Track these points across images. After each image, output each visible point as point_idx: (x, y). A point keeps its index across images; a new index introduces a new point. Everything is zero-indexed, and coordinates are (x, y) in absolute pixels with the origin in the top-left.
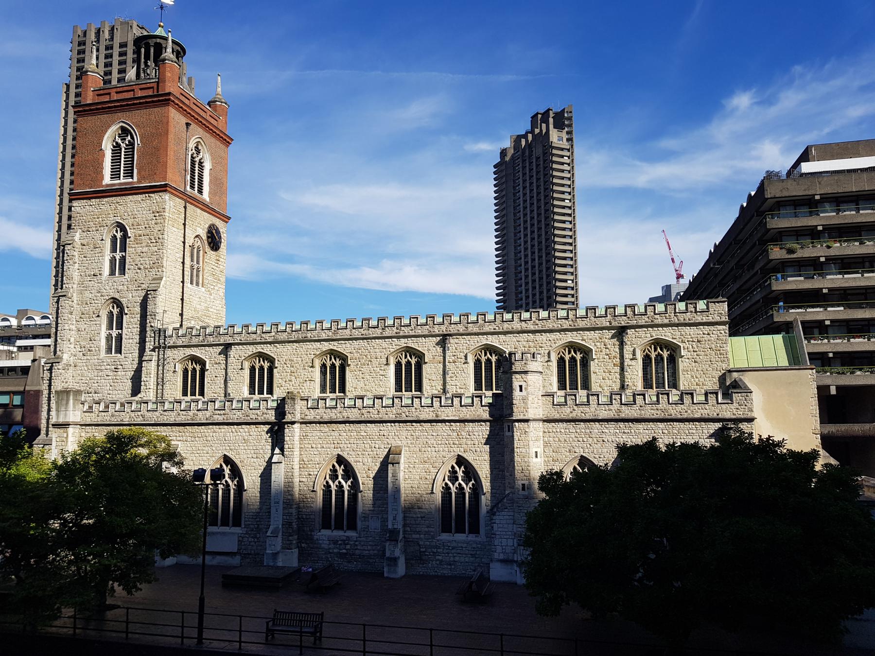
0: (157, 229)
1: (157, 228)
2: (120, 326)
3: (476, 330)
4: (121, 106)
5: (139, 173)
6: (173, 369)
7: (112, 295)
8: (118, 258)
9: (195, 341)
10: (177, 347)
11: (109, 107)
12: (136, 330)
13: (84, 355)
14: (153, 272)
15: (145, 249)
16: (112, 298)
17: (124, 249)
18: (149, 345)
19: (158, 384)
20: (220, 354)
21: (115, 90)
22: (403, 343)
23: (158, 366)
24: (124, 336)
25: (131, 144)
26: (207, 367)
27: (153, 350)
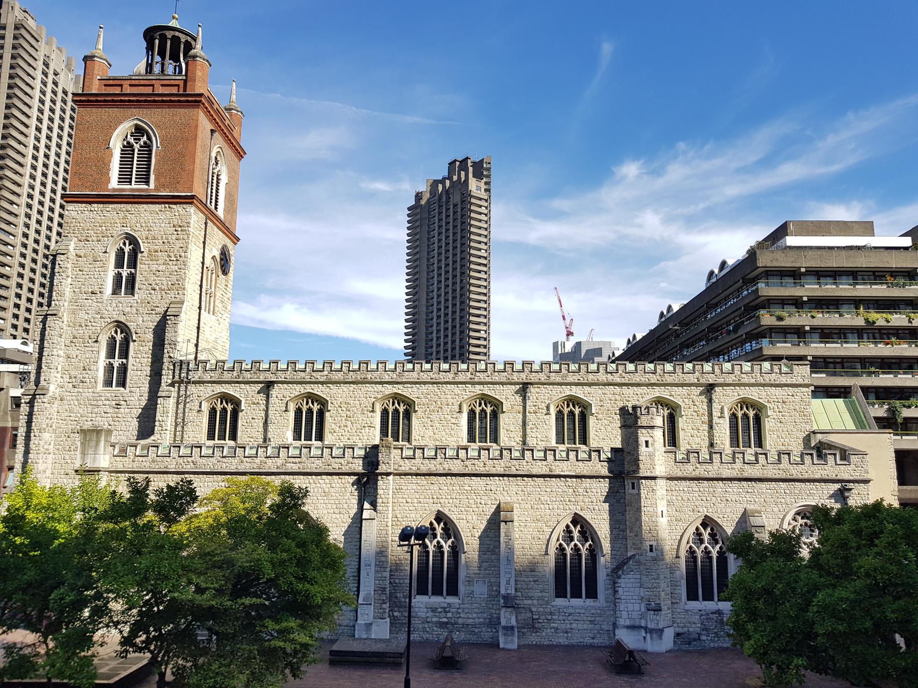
0: (178, 246)
1: (179, 244)
2: (125, 354)
4: (138, 101)
5: (156, 179)
6: (197, 408)
7: (116, 318)
8: (124, 274)
9: (227, 376)
10: (203, 382)
11: (121, 101)
12: (147, 360)
13: (74, 387)
14: (172, 294)
15: (161, 268)
16: (116, 321)
17: (133, 264)
18: (166, 378)
19: (176, 425)
20: (259, 393)
21: (129, 82)
22: (478, 390)
23: (178, 403)
24: (130, 367)
25: (148, 147)
26: (243, 408)
27: (172, 385)
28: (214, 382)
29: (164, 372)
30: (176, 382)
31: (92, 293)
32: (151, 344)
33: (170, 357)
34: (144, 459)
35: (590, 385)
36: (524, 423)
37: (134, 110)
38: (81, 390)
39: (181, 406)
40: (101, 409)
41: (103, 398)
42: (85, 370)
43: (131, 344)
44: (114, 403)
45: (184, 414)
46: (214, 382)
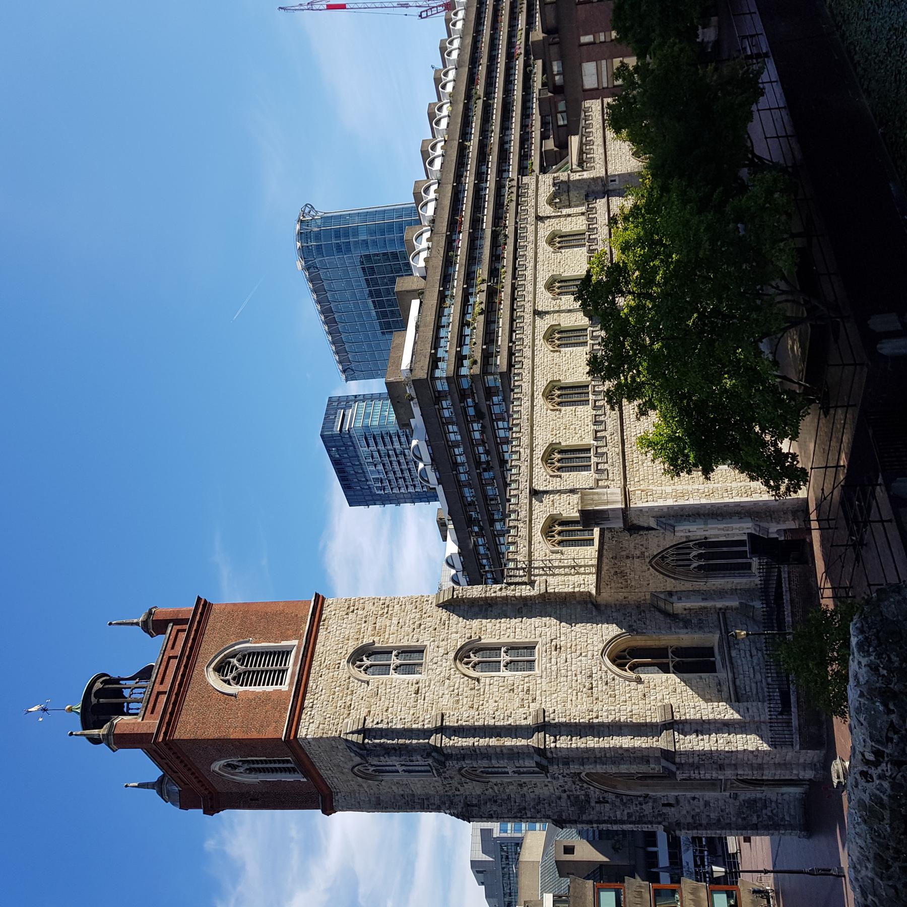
1: (369, 606)
2: (495, 649)
3: (531, 296)
4: (186, 667)
6: (558, 556)
7: (450, 662)
10: (530, 553)
11: (180, 685)
13: (534, 700)
14: (426, 607)
16: (455, 659)
18: (525, 591)
19: (578, 573)
20: (542, 502)
22: (540, 341)
23: (554, 575)
25: (245, 656)
27: (532, 583)
29: (518, 594)
30: (530, 578)
31: (417, 692)
32: (484, 621)
33: (501, 589)
34: (610, 472)
35: (535, 278)
36: (570, 311)
37: (195, 672)
38: (538, 692)
39: (557, 571)
40: (561, 664)
41: (548, 665)
42: (513, 690)
43: (483, 641)
44: (554, 653)
45: (564, 567)
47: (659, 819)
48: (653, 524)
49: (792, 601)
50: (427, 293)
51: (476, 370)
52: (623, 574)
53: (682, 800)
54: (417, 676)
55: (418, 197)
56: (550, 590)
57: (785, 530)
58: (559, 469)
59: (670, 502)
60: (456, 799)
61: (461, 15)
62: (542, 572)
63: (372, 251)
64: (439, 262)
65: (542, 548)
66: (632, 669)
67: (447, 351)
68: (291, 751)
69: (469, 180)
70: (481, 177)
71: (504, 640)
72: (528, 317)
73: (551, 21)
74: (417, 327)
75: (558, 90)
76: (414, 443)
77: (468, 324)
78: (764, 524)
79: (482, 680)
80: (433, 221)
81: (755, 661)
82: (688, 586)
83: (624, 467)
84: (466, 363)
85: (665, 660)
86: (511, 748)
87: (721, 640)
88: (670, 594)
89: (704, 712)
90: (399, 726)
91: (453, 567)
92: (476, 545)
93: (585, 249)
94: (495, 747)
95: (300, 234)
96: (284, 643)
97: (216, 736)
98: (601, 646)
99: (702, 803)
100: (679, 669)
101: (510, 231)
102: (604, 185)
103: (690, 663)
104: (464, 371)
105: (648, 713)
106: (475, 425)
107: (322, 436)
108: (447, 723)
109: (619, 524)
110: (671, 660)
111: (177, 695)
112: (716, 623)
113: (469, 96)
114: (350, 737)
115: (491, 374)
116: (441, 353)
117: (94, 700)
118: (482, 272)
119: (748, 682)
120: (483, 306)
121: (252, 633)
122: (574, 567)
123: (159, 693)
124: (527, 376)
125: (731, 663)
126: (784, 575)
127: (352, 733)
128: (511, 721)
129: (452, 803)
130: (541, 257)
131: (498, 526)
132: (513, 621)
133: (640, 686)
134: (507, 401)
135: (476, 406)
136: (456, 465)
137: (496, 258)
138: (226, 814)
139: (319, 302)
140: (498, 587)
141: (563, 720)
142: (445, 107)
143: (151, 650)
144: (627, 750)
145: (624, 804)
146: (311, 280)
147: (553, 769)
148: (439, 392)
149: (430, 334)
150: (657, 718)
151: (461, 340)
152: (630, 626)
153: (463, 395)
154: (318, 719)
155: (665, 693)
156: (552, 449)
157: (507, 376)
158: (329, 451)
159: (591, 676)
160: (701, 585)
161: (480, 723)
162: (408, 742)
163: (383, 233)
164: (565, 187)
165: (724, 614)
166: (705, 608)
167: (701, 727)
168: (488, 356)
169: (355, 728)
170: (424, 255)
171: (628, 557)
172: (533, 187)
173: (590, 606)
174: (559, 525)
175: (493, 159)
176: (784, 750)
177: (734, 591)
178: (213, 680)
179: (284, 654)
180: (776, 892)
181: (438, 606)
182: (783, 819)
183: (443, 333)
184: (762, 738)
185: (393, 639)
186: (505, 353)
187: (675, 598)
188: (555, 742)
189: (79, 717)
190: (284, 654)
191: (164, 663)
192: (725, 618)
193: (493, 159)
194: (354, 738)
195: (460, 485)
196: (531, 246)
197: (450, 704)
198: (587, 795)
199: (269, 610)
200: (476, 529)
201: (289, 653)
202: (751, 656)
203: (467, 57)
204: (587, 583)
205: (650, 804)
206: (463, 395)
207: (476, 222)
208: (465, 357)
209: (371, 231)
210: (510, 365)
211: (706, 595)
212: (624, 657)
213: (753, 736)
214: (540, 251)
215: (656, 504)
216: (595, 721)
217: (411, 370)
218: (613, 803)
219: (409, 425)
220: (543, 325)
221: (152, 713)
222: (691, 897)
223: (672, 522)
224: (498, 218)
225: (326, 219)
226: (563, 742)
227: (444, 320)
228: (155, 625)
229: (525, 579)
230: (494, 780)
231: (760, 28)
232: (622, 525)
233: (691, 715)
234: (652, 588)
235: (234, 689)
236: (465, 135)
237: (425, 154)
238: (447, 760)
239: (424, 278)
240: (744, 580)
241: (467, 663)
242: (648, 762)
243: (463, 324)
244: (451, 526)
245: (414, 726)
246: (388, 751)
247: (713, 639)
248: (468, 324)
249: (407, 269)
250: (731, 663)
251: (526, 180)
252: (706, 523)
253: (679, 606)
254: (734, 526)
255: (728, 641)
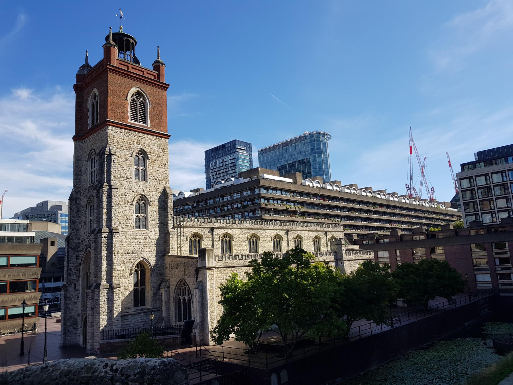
2: (146, 212)
3: (295, 229)
4: (139, 78)
6: (185, 239)
7: (140, 192)
10: (187, 227)
11: (131, 76)
13: (123, 228)
14: (164, 183)
15: (158, 169)
16: (141, 194)
18: (170, 225)
19: (178, 248)
22: (276, 232)
23: (177, 237)
25: (143, 104)
27: (174, 228)
28: (192, 227)
30: (176, 227)
31: (127, 178)
36: (288, 245)
39: (179, 239)
42: (127, 219)
45: (181, 242)
46: (192, 227)
47: (69, 282)
48: (199, 280)
49: (165, 339)
50: (295, 185)
51: (263, 206)
52: (177, 267)
53: (77, 292)
54: (134, 178)
55: (334, 182)
56: (171, 236)
57: (195, 336)
58: (222, 240)
59: (208, 287)
60: (79, 194)
61: (408, 201)
62: (178, 232)
63: (312, 163)
64: (308, 191)
65: (189, 232)
66: (136, 270)
67: (272, 194)
68: (102, 123)
69: (341, 204)
70: (342, 209)
71: (149, 216)
72: (286, 227)
73: (405, 238)
74: (281, 181)
75: (378, 241)
76: (233, 179)
77: (282, 203)
78: (198, 327)
79: (132, 206)
80: (324, 188)
81: (139, 324)
82: (172, 294)
83: (224, 267)
84: (266, 201)
85: (139, 285)
86: (102, 218)
87: (148, 309)
88: (168, 287)
89: (117, 302)
90: (112, 170)
91: (179, 195)
92: (188, 205)
93: (313, 251)
94: (102, 211)
95: (319, 133)
96: (149, 121)
97: (109, 91)
98: (146, 257)
99: (76, 301)
100: (135, 291)
101: (320, 220)
102: (340, 259)
103: (138, 296)
104: (263, 201)
105: (117, 278)
106: (240, 205)
107: (235, 140)
108: (113, 190)
109: (199, 265)
110: (139, 287)
111: (127, 74)
112: (155, 307)
113: (375, 204)
114: (107, 148)
115: (261, 212)
116: (270, 191)
117: (125, 38)
118: (304, 209)
119: (129, 320)
120: (290, 209)
121: (153, 108)
122: (180, 246)
123: (128, 67)
124: (261, 227)
125: (138, 313)
126: (176, 336)
127: (110, 149)
128: (114, 218)
129: (78, 192)
130: (310, 233)
131: (196, 214)
132: (158, 220)
133: (128, 274)
134: (251, 218)
135: (248, 205)
136: (223, 197)
137: (309, 215)
138: (74, 94)
139: (291, 140)
140: (172, 213)
141: (114, 241)
142: (370, 194)
143: (146, 63)
144: (101, 268)
145: (76, 267)
146: (300, 137)
147: (92, 236)
148: (254, 190)
149: (278, 186)
150: (114, 281)
151: (275, 199)
152: (154, 270)
153: (253, 200)
154: (116, 135)
155: (125, 285)
156: (231, 237)
157: (261, 218)
158: (228, 143)
159: (133, 253)
160: (172, 300)
161: (113, 205)
162: (105, 173)
163: (319, 168)
164: (339, 243)
165: (159, 310)
166: (162, 302)
167: (110, 301)
168: (269, 211)
169: (111, 151)
170: (311, 184)
171: (185, 269)
172: (339, 230)
173: (164, 253)
174: (199, 240)
175: (349, 214)
176: (100, 336)
177: (169, 314)
178: (133, 90)
179: (144, 121)
180: (35, 334)
181: (164, 188)
182: (68, 336)
183: (279, 192)
184: (105, 326)
185: (151, 168)
186: (270, 218)
187: (166, 289)
188: (104, 237)
189: (117, 32)
190: (144, 121)
191: (141, 69)
192: (157, 311)
193: (349, 214)
194: (107, 150)
195: (214, 198)
196: (315, 229)
197: (121, 192)
198: (80, 251)
199: (163, 115)
200: (195, 205)
201: (145, 123)
202: (141, 322)
203: (391, 204)
204: (173, 251)
205: (76, 279)
206: (253, 200)
207: (324, 206)
208: (268, 201)
209: (320, 163)
210: (266, 220)
211: (168, 302)
212: (141, 267)
213: (106, 323)
214: (313, 233)
215: (208, 281)
216: (114, 255)
217: (263, 178)
218: (76, 262)
219: (240, 177)
220: (283, 234)
221: (120, 63)
222: (33, 296)
223: (200, 288)
224: (325, 216)
225: (325, 144)
226: (104, 241)
227: (284, 193)
228: (157, 66)
229: (175, 225)
230: (87, 211)
231: (403, 324)
232: (199, 266)
233: (116, 296)
234: (171, 279)
235: (129, 99)
236: (359, 202)
237: (352, 186)
238: (97, 190)
239: (301, 185)
240: (174, 319)
241: (139, 200)
242: (95, 277)
243: (282, 201)
244: (197, 194)
245: (112, 176)
246: (101, 165)
247: (149, 305)
248: (282, 203)
249: (305, 178)
250: (138, 313)
251: (342, 227)
252: (199, 302)
253: (163, 291)
254: (198, 314)
255: (148, 312)
